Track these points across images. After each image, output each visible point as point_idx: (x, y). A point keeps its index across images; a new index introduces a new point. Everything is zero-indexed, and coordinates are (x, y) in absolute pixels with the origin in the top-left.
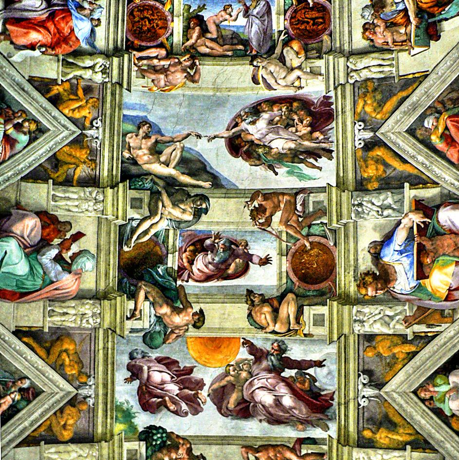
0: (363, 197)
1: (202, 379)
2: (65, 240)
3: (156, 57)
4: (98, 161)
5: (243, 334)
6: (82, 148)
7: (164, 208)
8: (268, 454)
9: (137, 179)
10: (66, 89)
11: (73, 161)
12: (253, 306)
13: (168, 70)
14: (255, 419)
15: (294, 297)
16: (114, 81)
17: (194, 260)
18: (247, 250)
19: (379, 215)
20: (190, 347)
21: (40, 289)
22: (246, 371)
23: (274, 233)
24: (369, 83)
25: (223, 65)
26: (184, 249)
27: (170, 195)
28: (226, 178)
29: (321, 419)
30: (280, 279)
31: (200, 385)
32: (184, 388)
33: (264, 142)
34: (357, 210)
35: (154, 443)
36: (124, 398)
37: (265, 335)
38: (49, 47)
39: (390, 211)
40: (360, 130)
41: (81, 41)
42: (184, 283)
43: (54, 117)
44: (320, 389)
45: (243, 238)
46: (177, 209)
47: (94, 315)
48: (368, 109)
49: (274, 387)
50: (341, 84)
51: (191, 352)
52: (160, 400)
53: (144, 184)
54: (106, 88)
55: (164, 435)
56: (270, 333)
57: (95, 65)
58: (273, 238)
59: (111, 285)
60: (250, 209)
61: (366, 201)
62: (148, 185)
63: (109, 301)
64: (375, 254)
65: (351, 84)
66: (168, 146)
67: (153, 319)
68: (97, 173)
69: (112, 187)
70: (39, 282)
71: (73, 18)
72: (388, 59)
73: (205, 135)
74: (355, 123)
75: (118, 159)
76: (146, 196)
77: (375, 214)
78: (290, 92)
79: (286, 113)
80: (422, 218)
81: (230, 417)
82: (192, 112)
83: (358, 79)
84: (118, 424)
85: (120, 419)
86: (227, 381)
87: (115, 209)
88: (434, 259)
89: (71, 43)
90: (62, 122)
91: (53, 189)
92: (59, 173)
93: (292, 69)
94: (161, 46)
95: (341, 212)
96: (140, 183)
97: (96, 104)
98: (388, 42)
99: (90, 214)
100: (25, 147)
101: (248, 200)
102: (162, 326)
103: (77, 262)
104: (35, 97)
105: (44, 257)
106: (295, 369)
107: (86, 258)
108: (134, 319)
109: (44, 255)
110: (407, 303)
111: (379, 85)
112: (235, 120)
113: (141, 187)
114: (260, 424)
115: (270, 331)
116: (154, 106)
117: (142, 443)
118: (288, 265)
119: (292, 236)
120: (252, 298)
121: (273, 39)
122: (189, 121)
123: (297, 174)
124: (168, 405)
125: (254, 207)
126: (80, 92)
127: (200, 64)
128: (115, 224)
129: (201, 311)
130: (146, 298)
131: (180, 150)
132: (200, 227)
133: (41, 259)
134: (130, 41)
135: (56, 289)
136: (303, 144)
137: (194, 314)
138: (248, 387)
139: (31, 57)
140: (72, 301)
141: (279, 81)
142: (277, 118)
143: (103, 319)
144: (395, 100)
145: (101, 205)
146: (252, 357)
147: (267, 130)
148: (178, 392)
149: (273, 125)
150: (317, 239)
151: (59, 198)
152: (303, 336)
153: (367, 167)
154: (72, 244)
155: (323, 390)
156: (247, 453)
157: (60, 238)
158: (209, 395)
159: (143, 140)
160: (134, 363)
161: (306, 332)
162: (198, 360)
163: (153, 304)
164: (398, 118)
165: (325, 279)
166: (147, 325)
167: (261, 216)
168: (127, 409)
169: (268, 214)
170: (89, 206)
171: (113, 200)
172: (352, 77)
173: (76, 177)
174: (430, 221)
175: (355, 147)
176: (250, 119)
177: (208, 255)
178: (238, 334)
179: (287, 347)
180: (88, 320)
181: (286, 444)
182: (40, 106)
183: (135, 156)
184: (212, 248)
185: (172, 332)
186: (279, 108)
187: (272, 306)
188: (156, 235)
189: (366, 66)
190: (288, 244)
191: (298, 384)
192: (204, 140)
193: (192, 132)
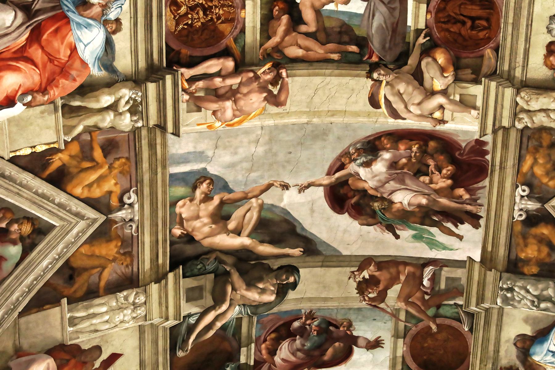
9: (195, 262)
16: (152, 123)
33: (382, 193)
41: (90, 66)
53: (204, 266)
62: (210, 267)
69: (158, 281)
71: (73, 26)
75: (165, 241)
96: (199, 267)
97: (126, 167)
112: (341, 160)
113: (202, 270)
116: (216, 151)
134: (173, 50)
136: (438, 201)
142: (404, 161)
147: (387, 176)
149: (396, 169)
159: (202, 204)
176: (363, 159)
183: (190, 230)
186: (407, 146)
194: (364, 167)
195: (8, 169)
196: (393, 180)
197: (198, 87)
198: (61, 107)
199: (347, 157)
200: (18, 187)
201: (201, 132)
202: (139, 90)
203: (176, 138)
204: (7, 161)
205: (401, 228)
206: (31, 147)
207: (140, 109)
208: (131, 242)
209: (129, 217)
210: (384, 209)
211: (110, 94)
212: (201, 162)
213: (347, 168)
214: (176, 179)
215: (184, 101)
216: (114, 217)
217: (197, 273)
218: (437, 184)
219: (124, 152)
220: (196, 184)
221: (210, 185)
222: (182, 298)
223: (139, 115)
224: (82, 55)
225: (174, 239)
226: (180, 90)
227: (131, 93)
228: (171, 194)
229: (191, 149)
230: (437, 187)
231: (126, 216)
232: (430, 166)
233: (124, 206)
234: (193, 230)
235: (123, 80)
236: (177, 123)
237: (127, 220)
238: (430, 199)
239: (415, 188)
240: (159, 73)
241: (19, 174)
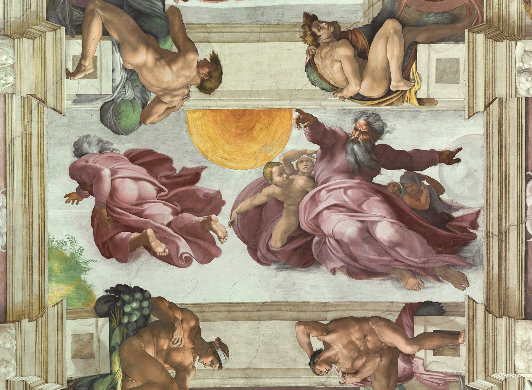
1: (219, 192)
5: (299, 103)
8: (349, 334)
12: (318, 45)
14: (324, 268)
20: (194, 130)
22: (303, 174)
29: (454, 266)
31: (214, 203)
32: (182, 212)
35: (126, 320)
36: (65, 233)
44: (451, 208)
49: (360, 205)
51: (196, 139)
52: (136, 234)
55: (146, 304)
56: (351, 98)
67: (120, 75)
81: (273, 266)
84: (53, 285)
85: (58, 274)
86: (268, 196)
102: (138, 89)
106: (399, 168)
108: (82, 75)
114: (332, 277)
115: (351, 95)
117: (101, 320)
120: (315, 30)
124: (153, 244)
129: (215, 60)
130: (105, 33)
137: (201, 65)
138: (308, 208)
143: (19, 76)
146: (317, 147)
148: (171, 218)
152: (416, 102)
155: (457, 209)
156: (308, 335)
158: (232, 224)
160: (83, 163)
161: (422, 95)
162: (210, 154)
163: (119, 46)
166: (107, 89)
168: (73, 255)
178: (288, 103)
179: (384, 125)
181: (382, 315)
185: (158, 100)
191: (406, 199)
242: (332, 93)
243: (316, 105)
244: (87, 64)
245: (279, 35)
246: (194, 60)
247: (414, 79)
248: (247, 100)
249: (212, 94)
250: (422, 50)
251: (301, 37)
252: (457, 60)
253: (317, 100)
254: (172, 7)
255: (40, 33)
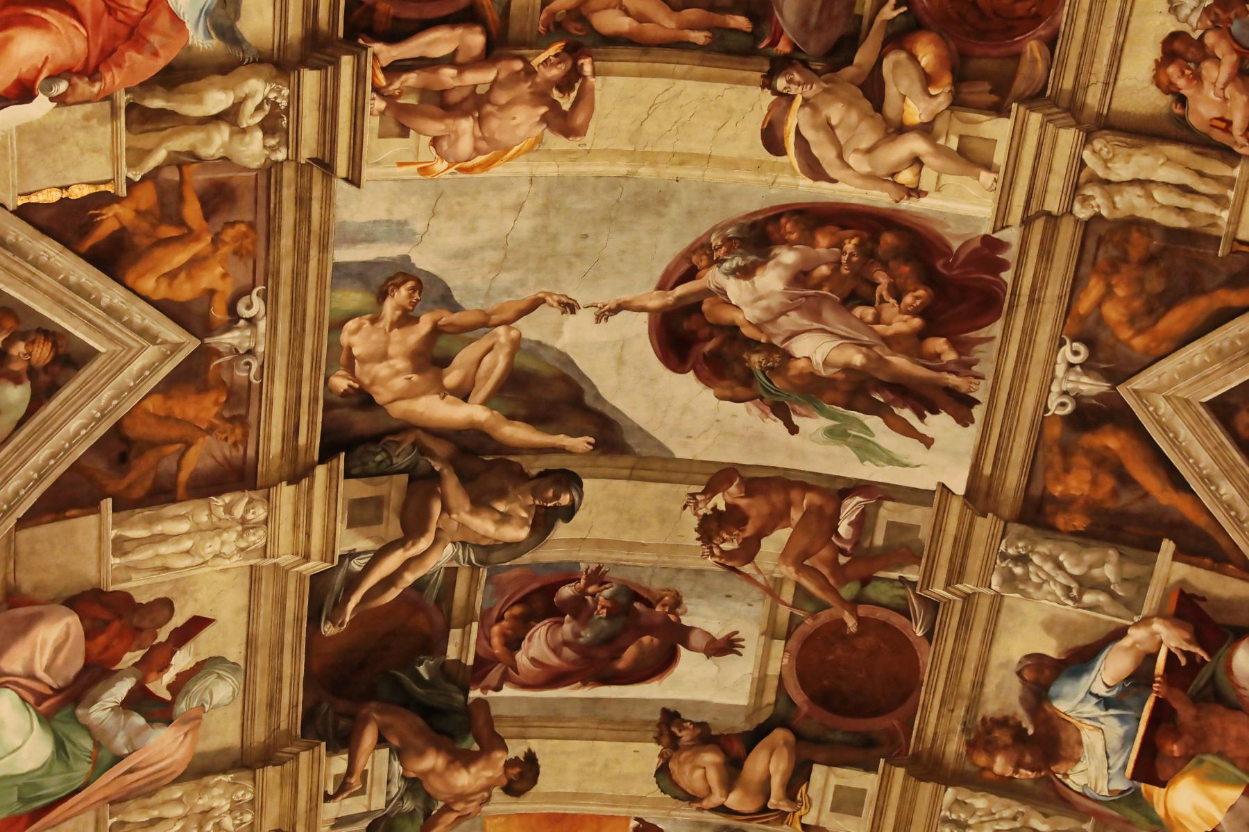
0: (1035, 543)
2: (153, 648)
3: (449, 60)
4: (252, 418)
6: (204, 389)
7: (446, 516)
9: (372, 448)
10: (143, 207)
11: (175, 432)
13: (489, 102)
15: (790, 737)
17: (524, 638)
18: (677, 615)
19: (1069, 597)
21: (86, 785)
23: (760, 579)
24: (1135, 236)
25: (671, 76)
26: (495, 614)
27: (466, 480)
28: (640, 429)
30: (759, 691)
33: (770, 336)
34: (1010, 571)
37: (698, 814)
38: (80, 74)
39: (1102, 598)
40: (1071, 366)
41: (189, 26)
42: (491, 694)
43: (111, 311)
45: (670, 586)
46: (486, 514)
47: (236, 807)
48: (1113, 312)
50: (1049, 214)
53: (390, 457)
54: (279, 184)
56: (713, 810)
57: (237, 108)
58: (756, 593)
59: (284, 726)
60: (701, 512)
61: (1038, 553)
62: (401, 461)
63: (279, 768)
64: (1036, 683)
65: (1077, 220)
66: (471, 341)
68: (251, 452)
69: (294, 480)
70: (83, 769)
72: (1217, 179)
73: (589, 303)
74: (1062, 343)
75: (314, 400)
76: (394, 488)
77: (1059, 592)
78: (880, 198)
79: (855, 259)
80: (1189, 642)
82: (551, 230)
83: (1104, 213)
87: (302, 536)
88: (1191, 752)
89: (155, 39)
90: (137, 320)
91: (114, 523)
92: (132, 476)
93: (899, 129)
94: (467, 17)
95: (963, 565)
96: (379, 458)
97: (247, 242)
98: (1230, 123)
99: (226, 563)
100: (21, 423)
101: (700, 489)
103: (188, 692)
104: (45, 258)
105: (95, 707)
107: (212, 678)
108: (345, 795)
109: (95, 702)
110: (1092, 820)
111: (1164, 249)
113: (384, 465)
118: (786, 661)
119: (810, 596)
120: (675, 730)
121: (857, 10)
122: (543, 259)
123: (858, 442)
125: (714, 509)
126: (192, 211)
127: (594, 74)
128: (300, 573)
129: (531, 758)
130: (381, 741)
131: (507, 350)
132: (548, 554)
133: (88, 715)
135: (131, 771)
136: (888, 362)
137: (509, 764)
139: (18, 128)
140: (174, 788)
141: (852, 159)
142: (824, 270)
144: (1200, 306)
145: (261, 533)
149: (807, 288)
150: (881, 614)
151: (135, 543)
152: (799, 827)
153: (1067, 470)
154: (173, 653)
157: (140, 648)
159: (396, 331)
164: (1197, 360)
165: (878, 713)
166: (378, 802)
167: (731, 534)
169: (750, 530)
170: (223, 543)
171: (296, 514)
172: (1086, 199)
173: (184, 476)
174: (1206, 657)
175: (1047, 410)
176: (737, 261)
177: (562, 623)
180: (218, 824)
182: (61, 282)
183: (367, 381)
184: (578, 608)
185: (447, 808)
187: (725, 751)
188: (419, 585)
189: (1142, 177)
190: (796, 612)
192: (585, 317)
193: (550, 294)
194: (738, 277)
195: (14, 229)
196: (795, 309)
197: (406, 84)
198: (126, 109)
199: (705, 253)
200: (30, 267)
201: (404, 180)
202: (285, 84)
203: (353, 189)
204: (12, 212)
205: (804, 412)
206: (61, 188)
207: (284, 123)
208: (245, 396)
209: (247, 345)
210: (771, 369)
211: (225, 89)
212: (400, 243)
213: (701, 278)
214: (345, 273)
215: (375, 112)
216: (215, 343)
217: (375, 471)
218: (889, 324)
219: (244, 212)
220: (385, 288)
221: (414, 292)
222: (339, 518)
223: (280, 136)
224: (175, 4)
225: (333, 397)
226: (369, 88)
227: (268, 88)
228: (335, 305)
229: (382, 215)
230: (890, 330)
231: (240, 343)
232: (878, 284)
233: (237, 322)
234: (373, 383)
235: (254, 61)
236: (357, 159)
237: (241, 352)
238: (871, 353)
239: (842, 329)
240: (329, 50)
241: (34, 242)
242: (687, 802)
243: (663, 814)
244: (353, 780)
245: (624, 734)
246: (502, 758)
247: (802, 802)
248: (568, 804)
249: (522, 796)
250: (818, 772)
251: (655, 738)
252: (864, 791)
253: (666, 809)
254: (478, 700)
255: (291, 756)
